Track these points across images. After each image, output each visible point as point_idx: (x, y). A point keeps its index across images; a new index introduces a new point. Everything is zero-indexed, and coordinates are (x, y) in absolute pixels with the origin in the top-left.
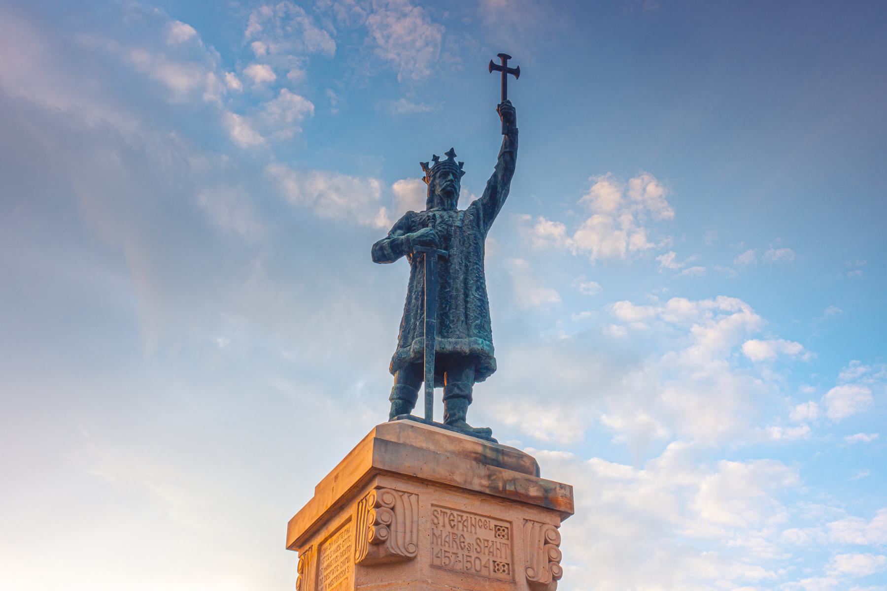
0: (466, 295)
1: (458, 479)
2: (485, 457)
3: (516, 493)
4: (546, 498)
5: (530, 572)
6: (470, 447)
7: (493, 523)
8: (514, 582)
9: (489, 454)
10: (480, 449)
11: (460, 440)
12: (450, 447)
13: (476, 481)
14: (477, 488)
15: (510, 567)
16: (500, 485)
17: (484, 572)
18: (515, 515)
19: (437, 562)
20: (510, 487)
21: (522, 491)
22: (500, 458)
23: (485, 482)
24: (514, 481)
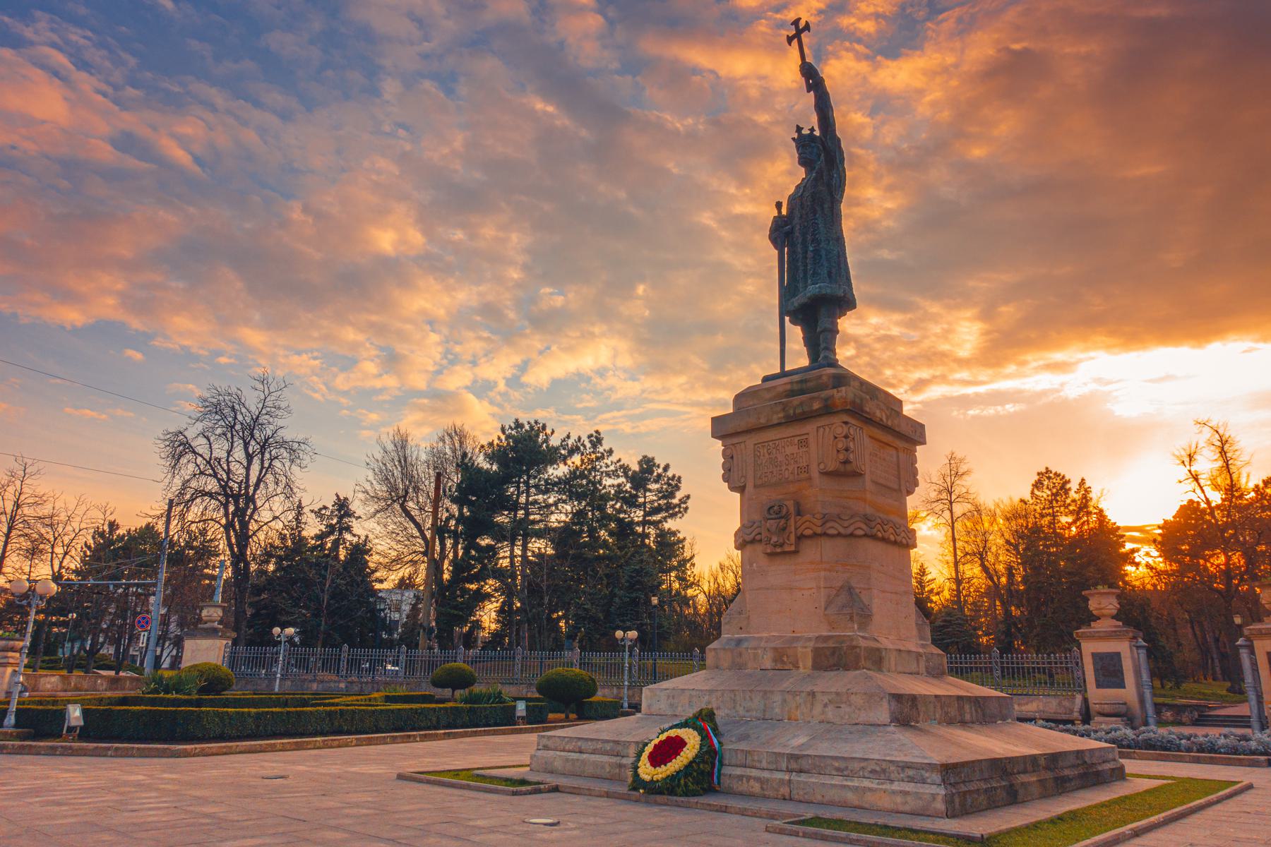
0: (806, 252)
1: (763, 421)
2: (792, 391)
3: (804, 413)
4: (826, 406)
5: (822, 466)
6: (780, 389)
7: (796, 439)
8: (810, 479)
9: (796, 387)
10: (788, 387)
11: (775, 387)
12: (768, 396)
13: (775, 417)
14: (776, 422)
15: (807, 469)
16: (791, 412)
17: (791, 478)
18: (810, 428)
19: (759, 482)
20: (799, 411)
21: (806, 409)
22: (804, 386)
23: (781, 415)
24: (801, 404)
